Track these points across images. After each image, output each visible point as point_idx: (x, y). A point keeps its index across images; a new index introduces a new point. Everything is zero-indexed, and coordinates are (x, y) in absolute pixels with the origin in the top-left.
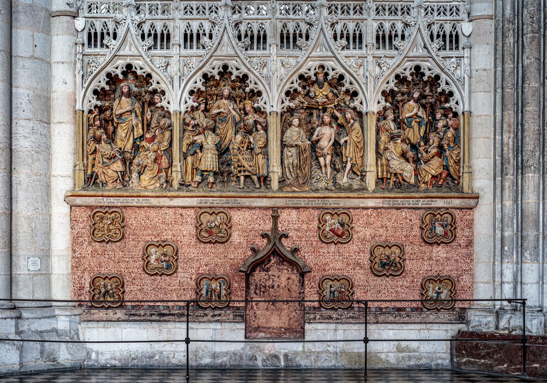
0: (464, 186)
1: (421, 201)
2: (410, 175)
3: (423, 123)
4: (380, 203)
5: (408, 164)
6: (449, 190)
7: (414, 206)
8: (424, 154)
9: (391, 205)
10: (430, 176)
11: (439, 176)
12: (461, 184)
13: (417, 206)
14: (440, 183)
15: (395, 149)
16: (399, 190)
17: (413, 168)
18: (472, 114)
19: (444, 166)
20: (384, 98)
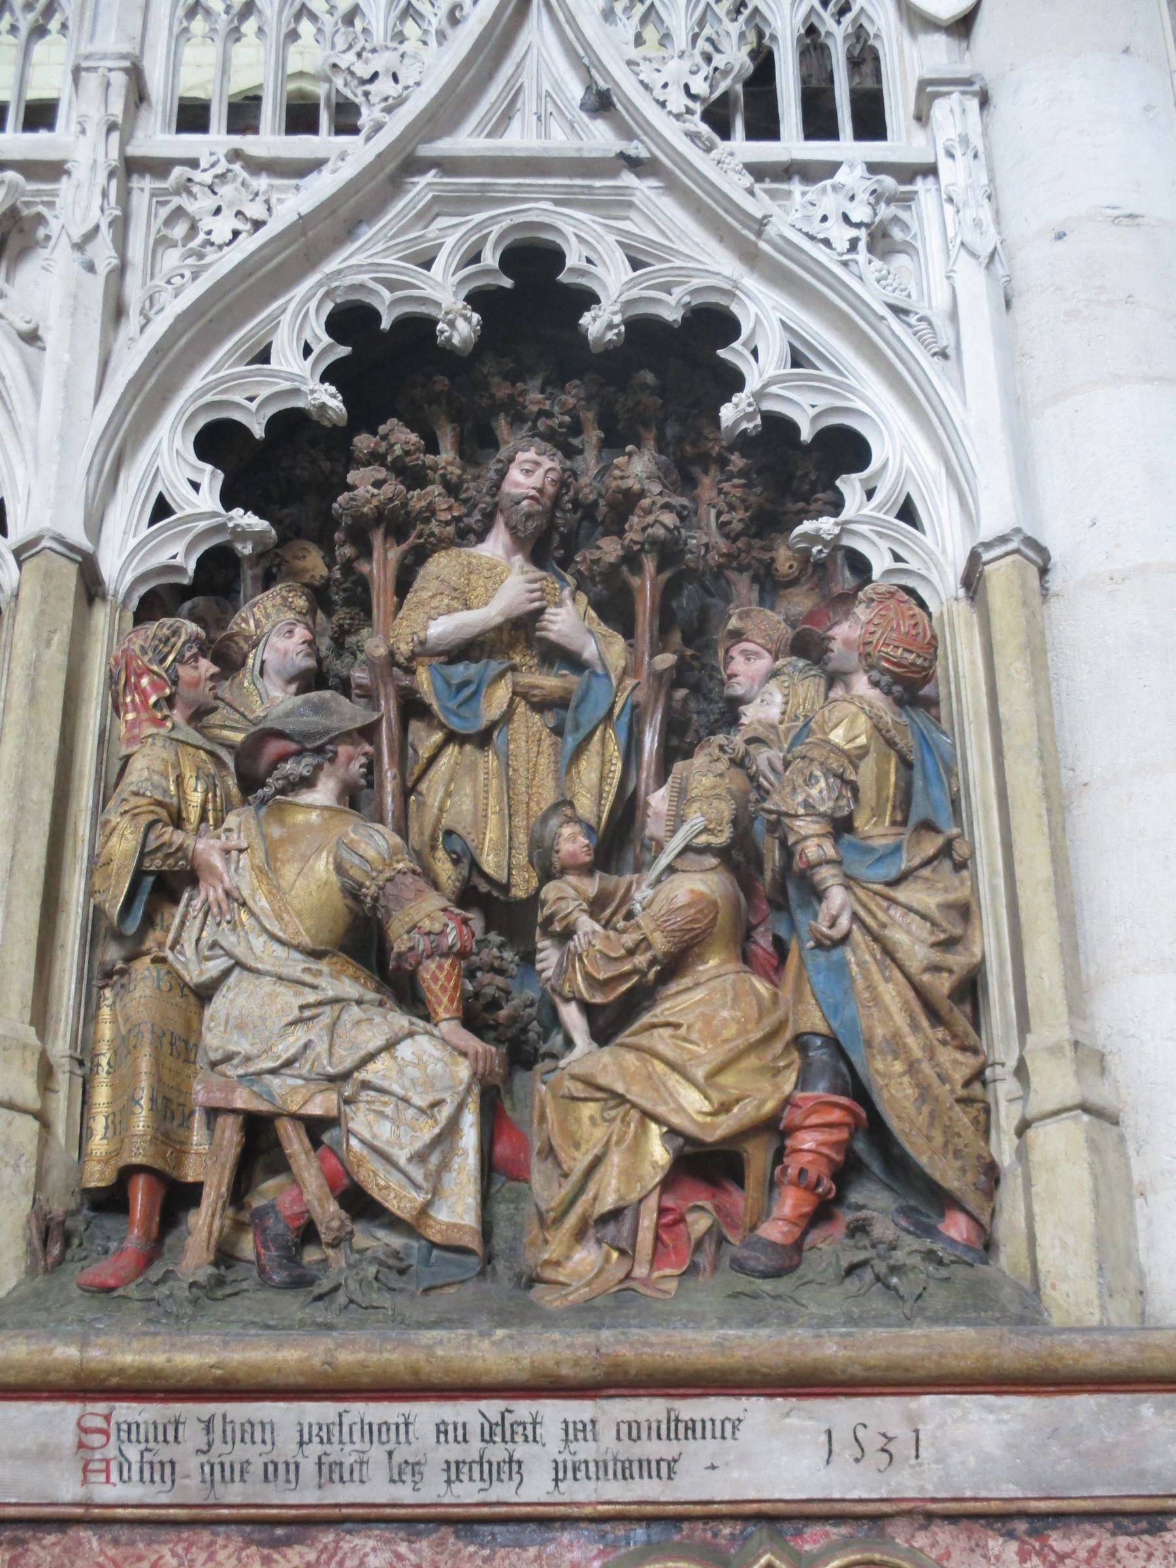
0: (1049, 1256)
1: (551, 1432)
2: (427, 1133)
3: (593, 711)
4: (44, 1454)
5: (401, 1020)
6: (878, 1302)
7: (468, 1492)
8: (586, 924)
9: (191, 1488)
10: (659, 1152)
11: (757, 1157)
12: (1011, 1254)
13: (503, 1491)
14: (774, 1231)
15: (268, 870)
16: (293, 1305)
17: (463, 1071)
18: (1055, 580)
19: (800, 1042)
20: (211, 478)
